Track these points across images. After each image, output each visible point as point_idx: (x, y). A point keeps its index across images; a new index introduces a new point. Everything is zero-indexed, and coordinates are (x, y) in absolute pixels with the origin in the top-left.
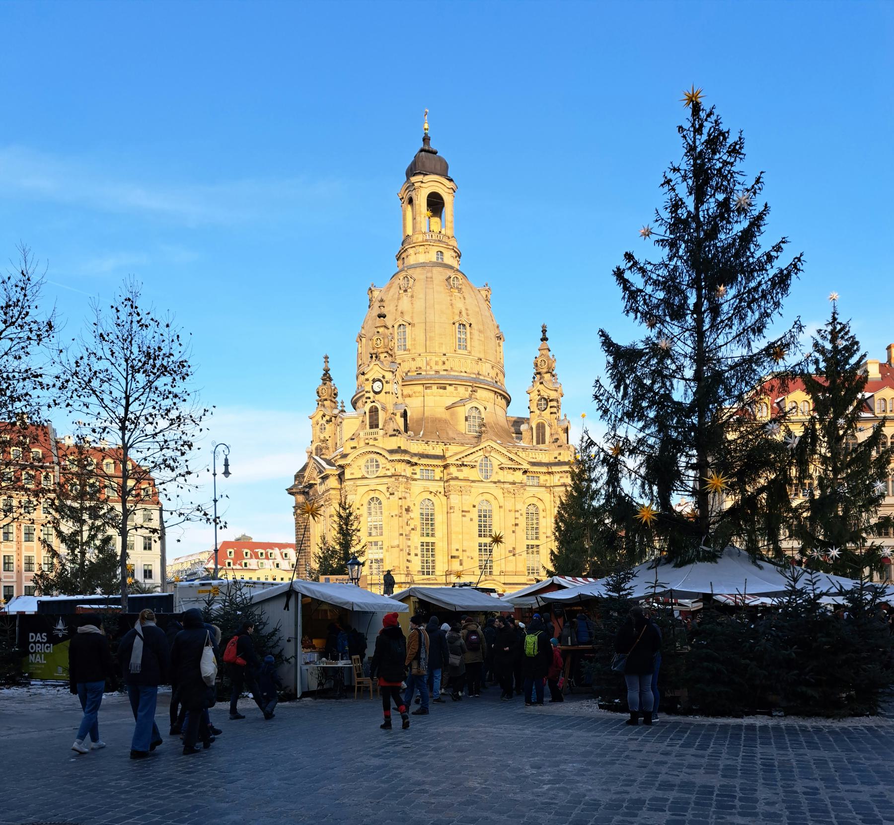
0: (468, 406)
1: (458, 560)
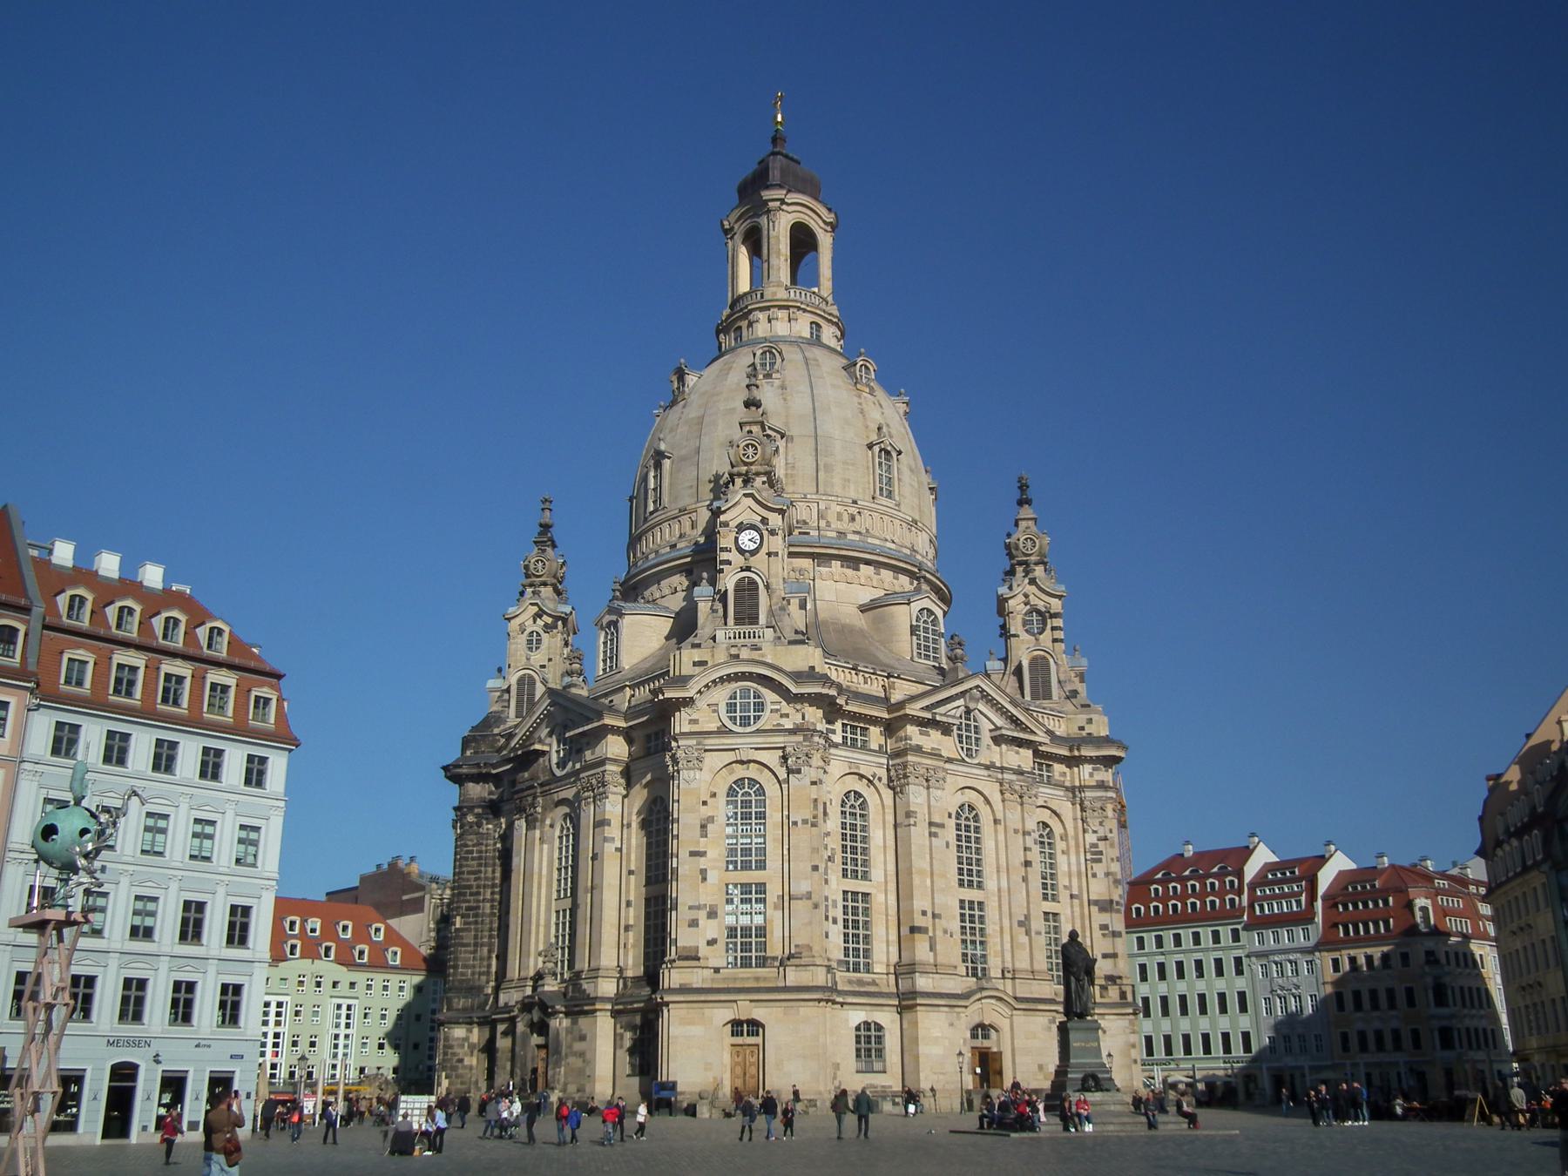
0: (916, 606)
1: (925, 937)
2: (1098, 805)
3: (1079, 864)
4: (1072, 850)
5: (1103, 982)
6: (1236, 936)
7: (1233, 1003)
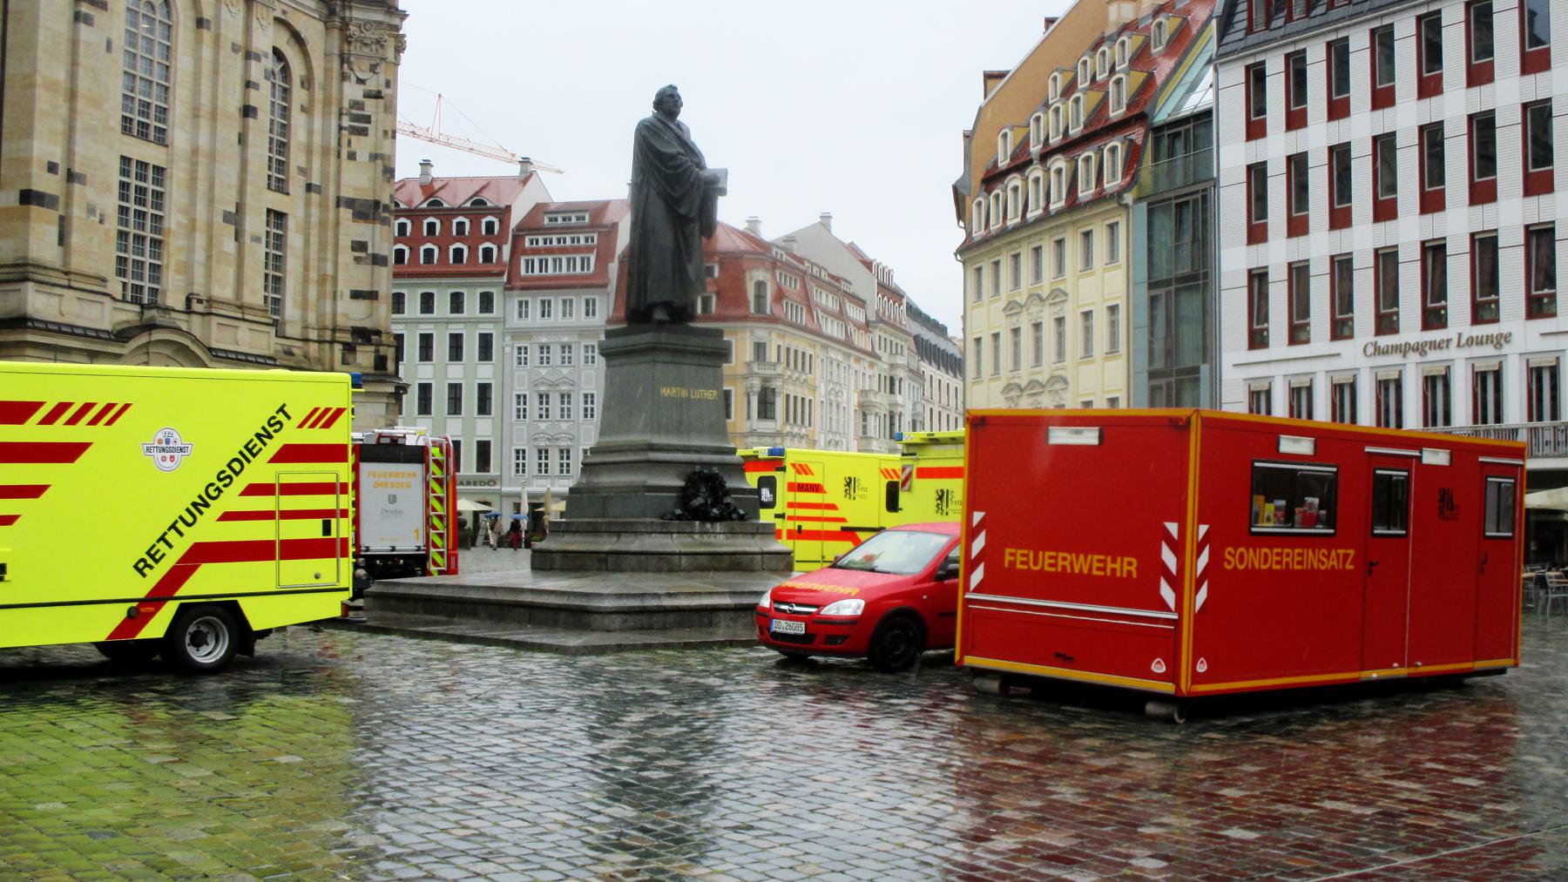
1: (54, 215)
2: (371, 35)
3: (325, 133)
4: (318, 108)
5: (348, 338)
6: (486, 302)
7: (470, 399)
